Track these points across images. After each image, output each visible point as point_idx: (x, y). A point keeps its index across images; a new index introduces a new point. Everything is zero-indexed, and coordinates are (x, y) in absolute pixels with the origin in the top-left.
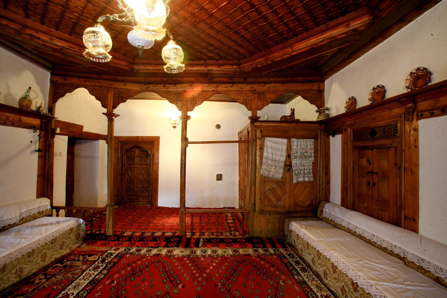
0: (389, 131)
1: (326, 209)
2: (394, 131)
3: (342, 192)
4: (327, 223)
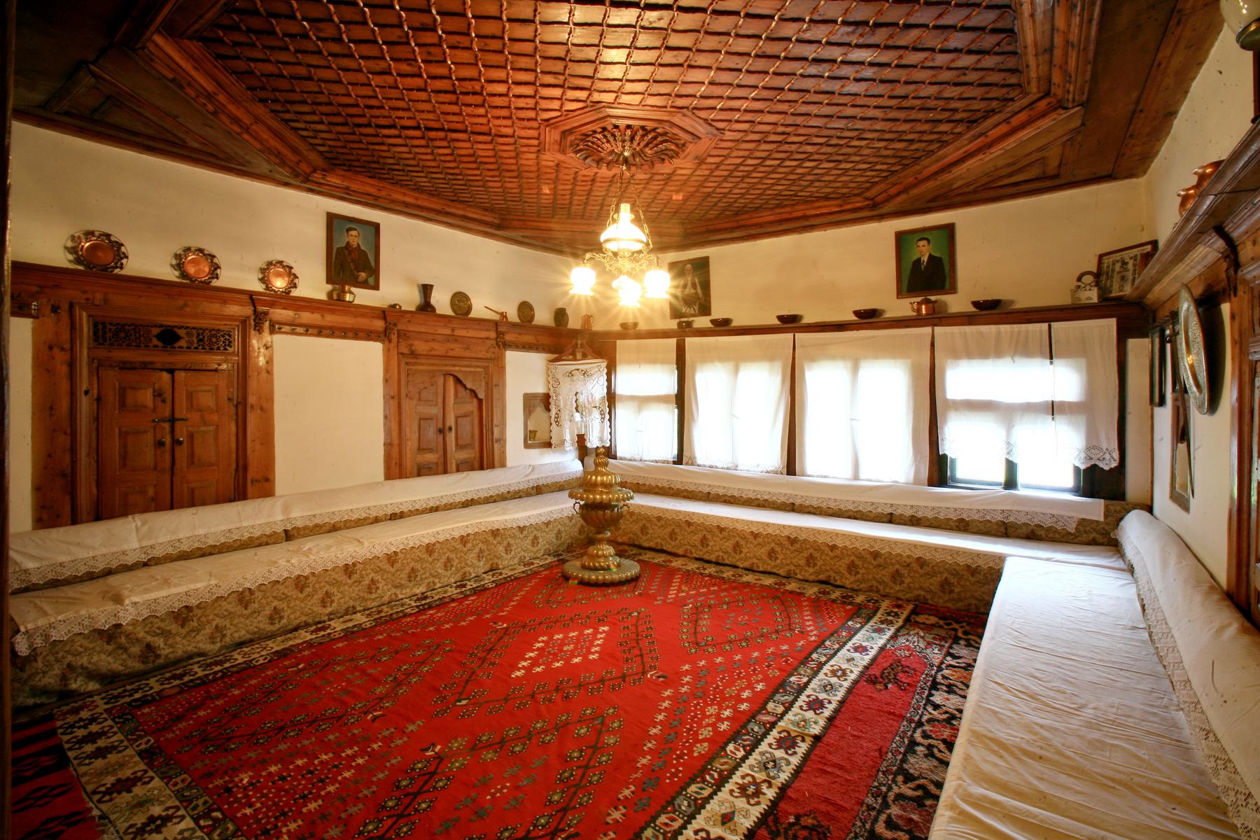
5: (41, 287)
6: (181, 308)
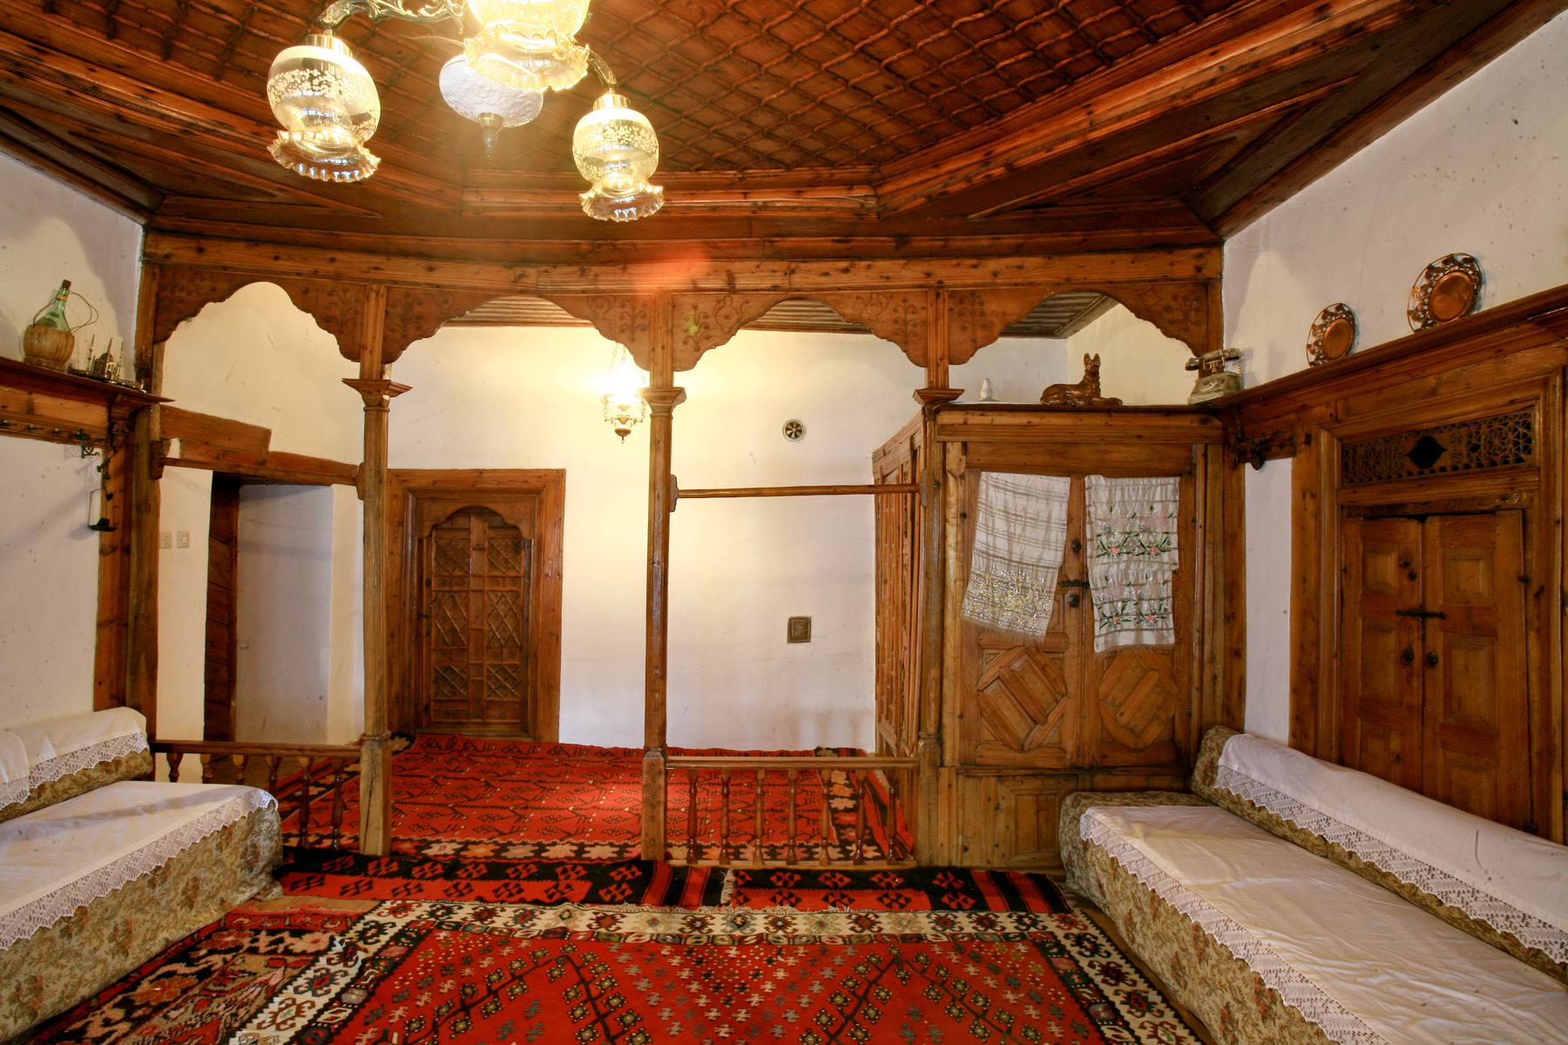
0: (1496, 442)
1: (1227, 759)
2: (1516, 444)
3: (1295, 691)
4: (1235, 814)
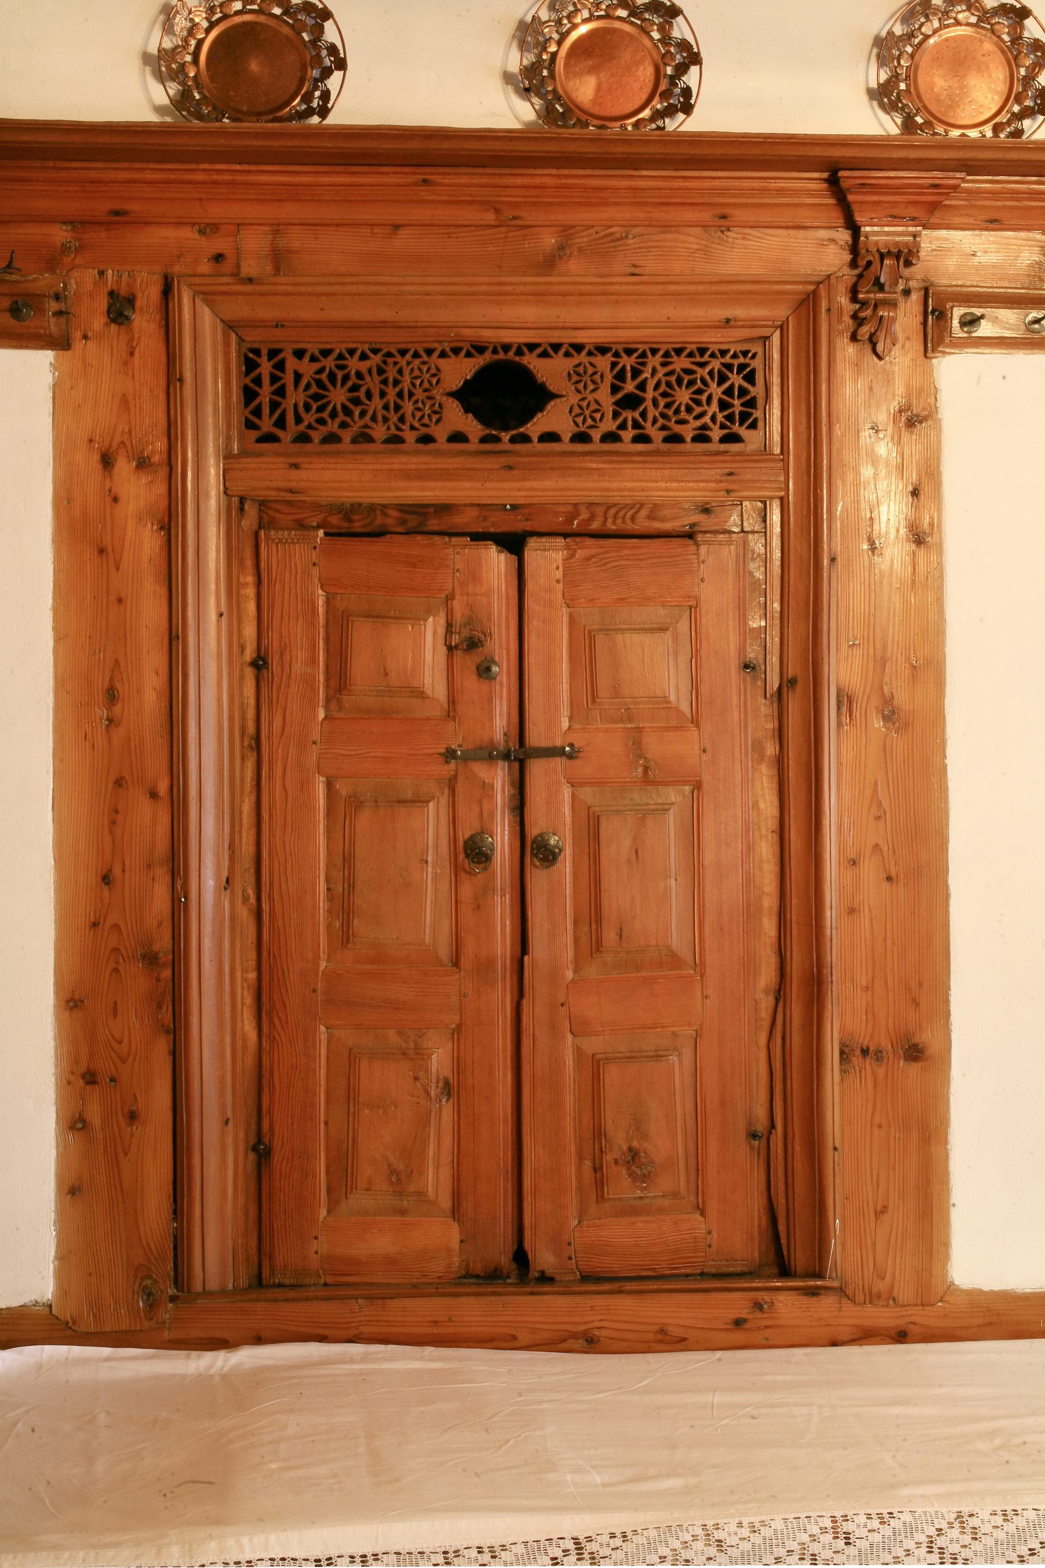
0: (683, 396)
5: (78, 224)
6: (549, 263)
